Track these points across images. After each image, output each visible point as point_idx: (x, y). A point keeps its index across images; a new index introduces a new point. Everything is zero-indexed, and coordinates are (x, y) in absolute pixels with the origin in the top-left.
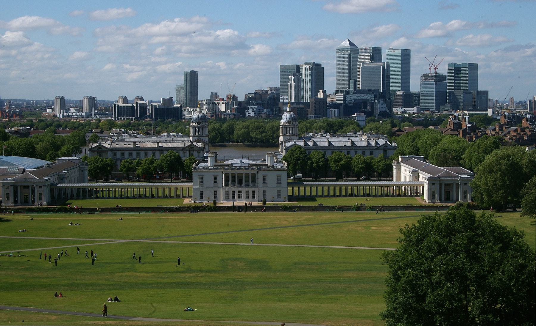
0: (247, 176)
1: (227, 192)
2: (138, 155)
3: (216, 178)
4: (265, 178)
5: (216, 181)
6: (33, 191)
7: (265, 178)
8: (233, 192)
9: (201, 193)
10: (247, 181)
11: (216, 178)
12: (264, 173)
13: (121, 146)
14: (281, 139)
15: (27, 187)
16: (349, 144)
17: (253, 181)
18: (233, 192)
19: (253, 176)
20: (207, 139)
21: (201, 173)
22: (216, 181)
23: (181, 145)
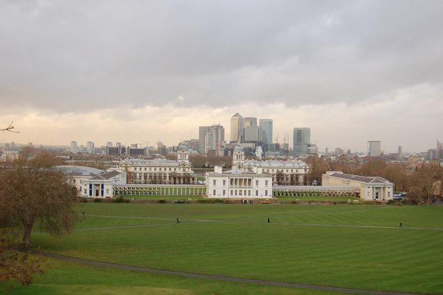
0: (245, 179)
1: (232, 191)
2: (150, 169)
3: (224, 181)
4: (257, 181)
5: (224, 184)
6: (103, 187)
7: (257, 181)
8: (236, 191)
9: (214, 191)
10: (245, 184)
11: (224, 181)
12: (257, 179)
13: (139, 164)
14: (234, 162)
15: (98, 185)
16: (282, 165)
17: (249, 184)
18: (236, 191)
19: (250, 180)
20: (187, 162)
21: (215, 178)
22: (224, 184)
23: (177, 164)
